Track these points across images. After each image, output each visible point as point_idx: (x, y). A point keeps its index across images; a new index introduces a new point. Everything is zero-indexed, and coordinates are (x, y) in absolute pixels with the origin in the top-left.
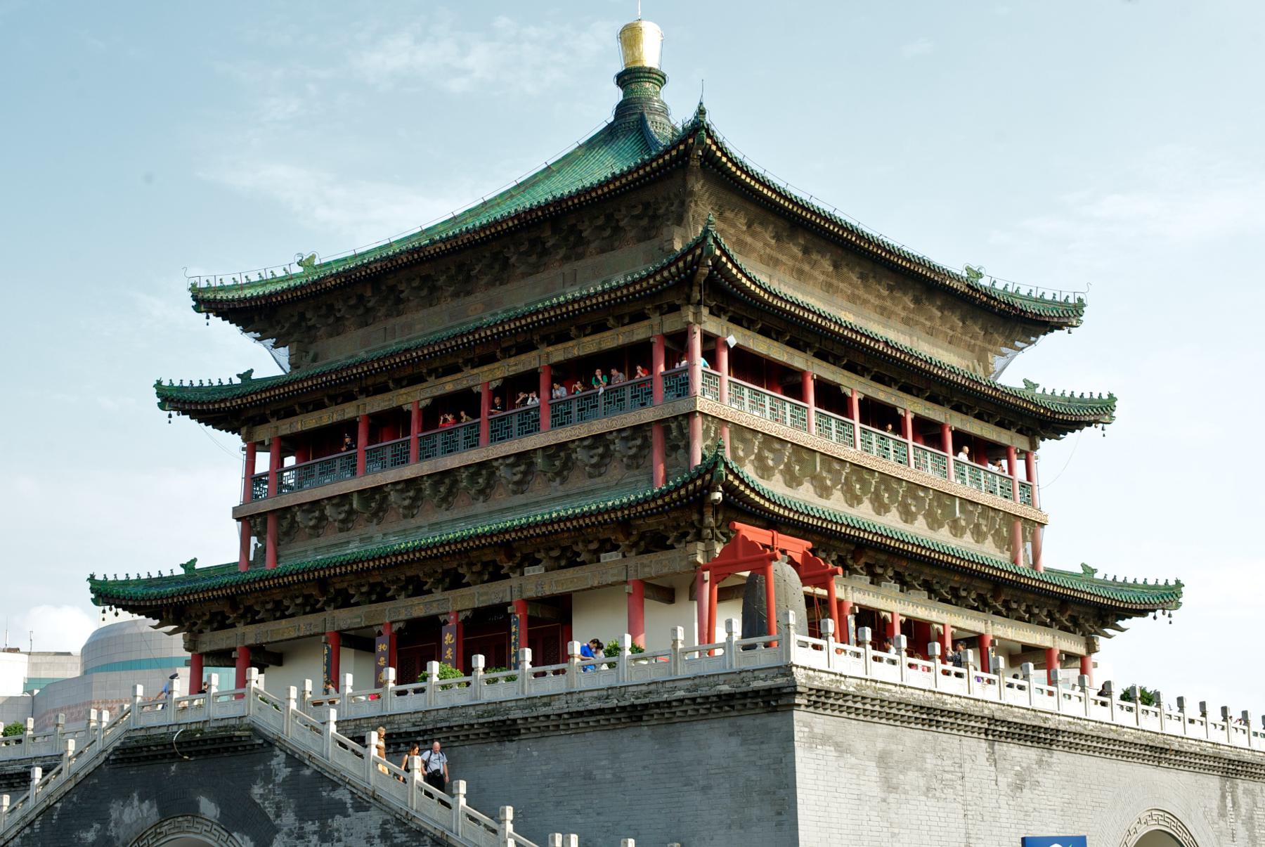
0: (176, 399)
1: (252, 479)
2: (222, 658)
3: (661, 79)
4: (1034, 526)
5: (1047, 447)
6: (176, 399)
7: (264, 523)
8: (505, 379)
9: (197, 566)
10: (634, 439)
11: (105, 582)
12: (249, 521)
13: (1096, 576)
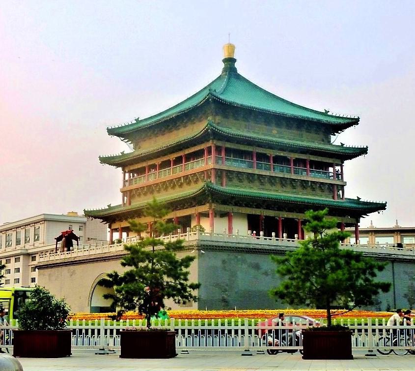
0: (105, 160)
1: (125, 181)
2: (116, 230)
3: (235, 60)
4: (342, 187)
5: (347, 163)
6: (105, 160)
7: (127, 193)
8: (176, 158)
9: (111, 206)
12: (124, 193)
13: (360, 200)
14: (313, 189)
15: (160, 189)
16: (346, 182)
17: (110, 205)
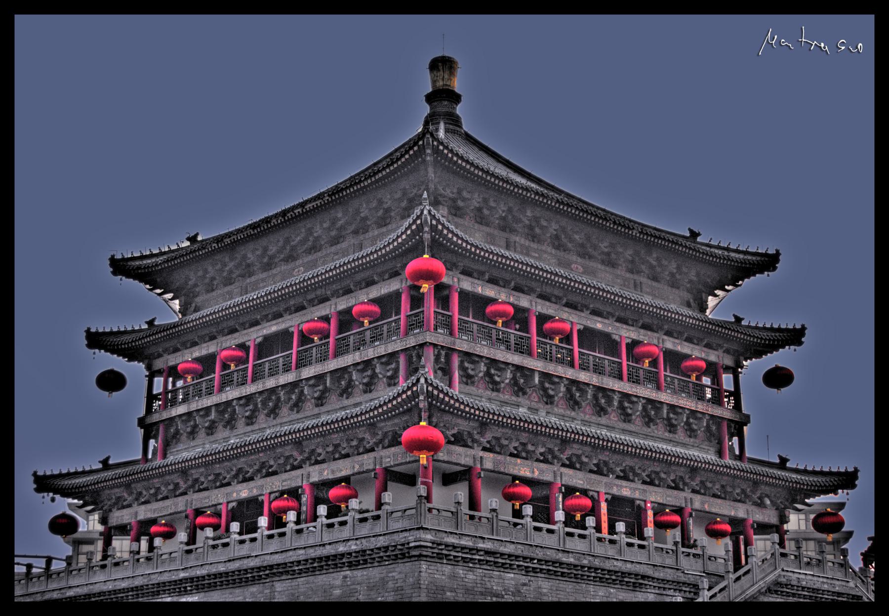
1: (151, 398)
10: (389, 364)
11: (45, 477)
14: (671, 427)
15: (255, 410)
16: (748, 417)
17: (108, 458)
